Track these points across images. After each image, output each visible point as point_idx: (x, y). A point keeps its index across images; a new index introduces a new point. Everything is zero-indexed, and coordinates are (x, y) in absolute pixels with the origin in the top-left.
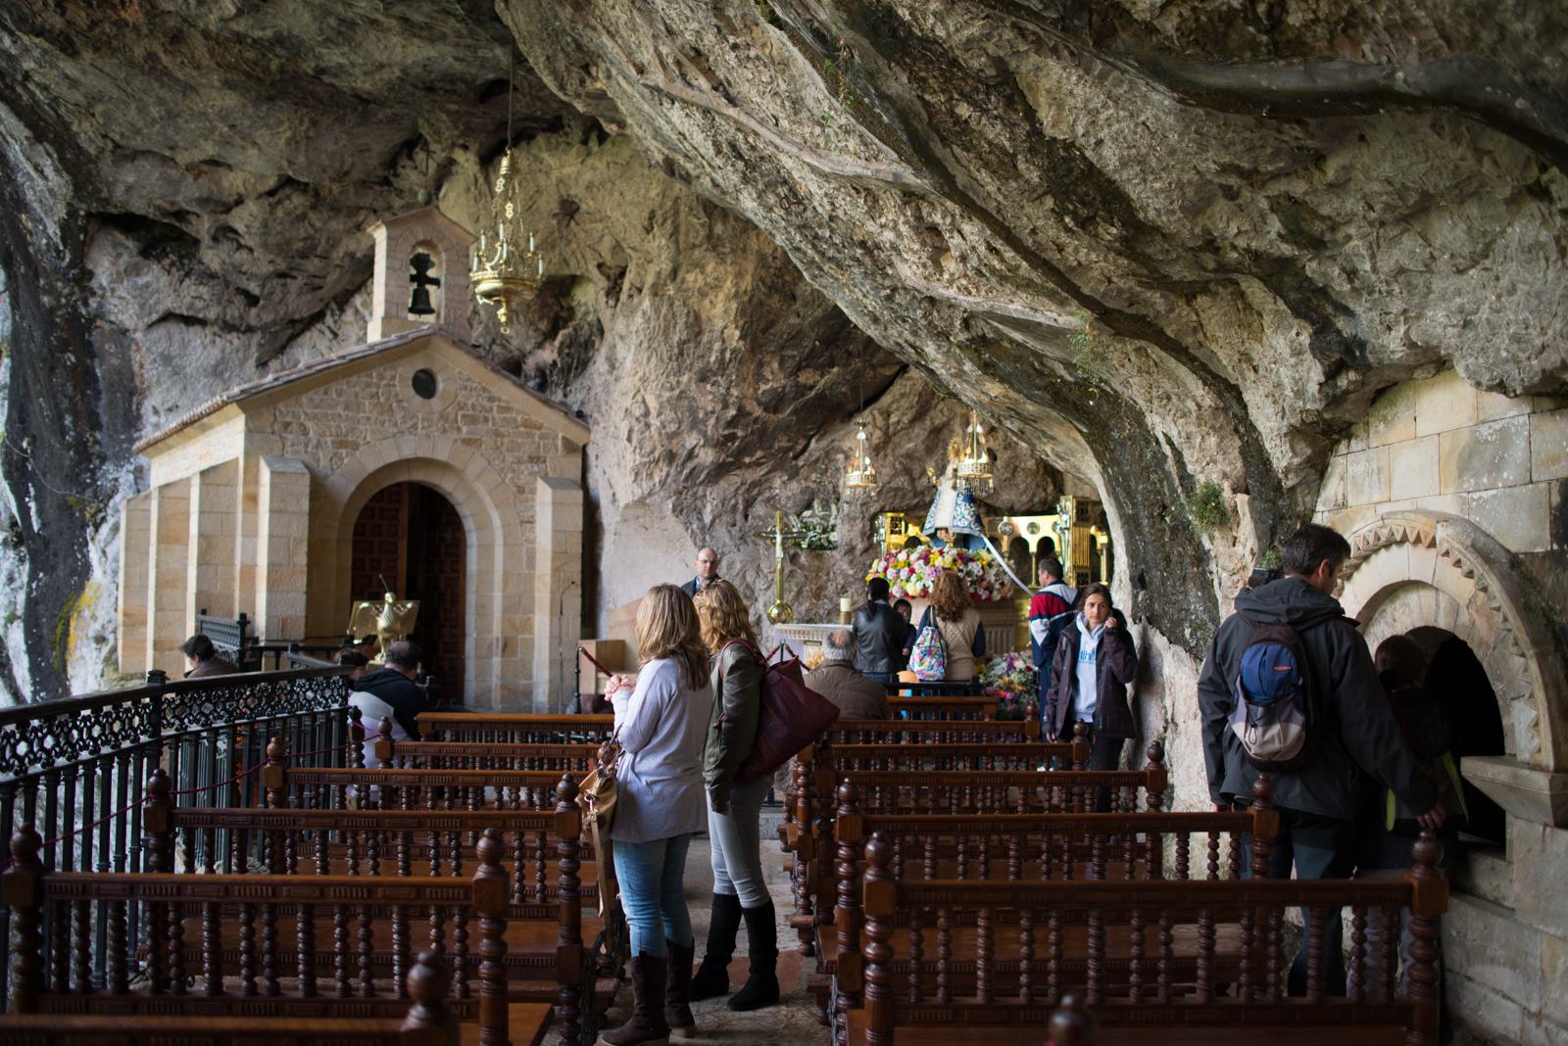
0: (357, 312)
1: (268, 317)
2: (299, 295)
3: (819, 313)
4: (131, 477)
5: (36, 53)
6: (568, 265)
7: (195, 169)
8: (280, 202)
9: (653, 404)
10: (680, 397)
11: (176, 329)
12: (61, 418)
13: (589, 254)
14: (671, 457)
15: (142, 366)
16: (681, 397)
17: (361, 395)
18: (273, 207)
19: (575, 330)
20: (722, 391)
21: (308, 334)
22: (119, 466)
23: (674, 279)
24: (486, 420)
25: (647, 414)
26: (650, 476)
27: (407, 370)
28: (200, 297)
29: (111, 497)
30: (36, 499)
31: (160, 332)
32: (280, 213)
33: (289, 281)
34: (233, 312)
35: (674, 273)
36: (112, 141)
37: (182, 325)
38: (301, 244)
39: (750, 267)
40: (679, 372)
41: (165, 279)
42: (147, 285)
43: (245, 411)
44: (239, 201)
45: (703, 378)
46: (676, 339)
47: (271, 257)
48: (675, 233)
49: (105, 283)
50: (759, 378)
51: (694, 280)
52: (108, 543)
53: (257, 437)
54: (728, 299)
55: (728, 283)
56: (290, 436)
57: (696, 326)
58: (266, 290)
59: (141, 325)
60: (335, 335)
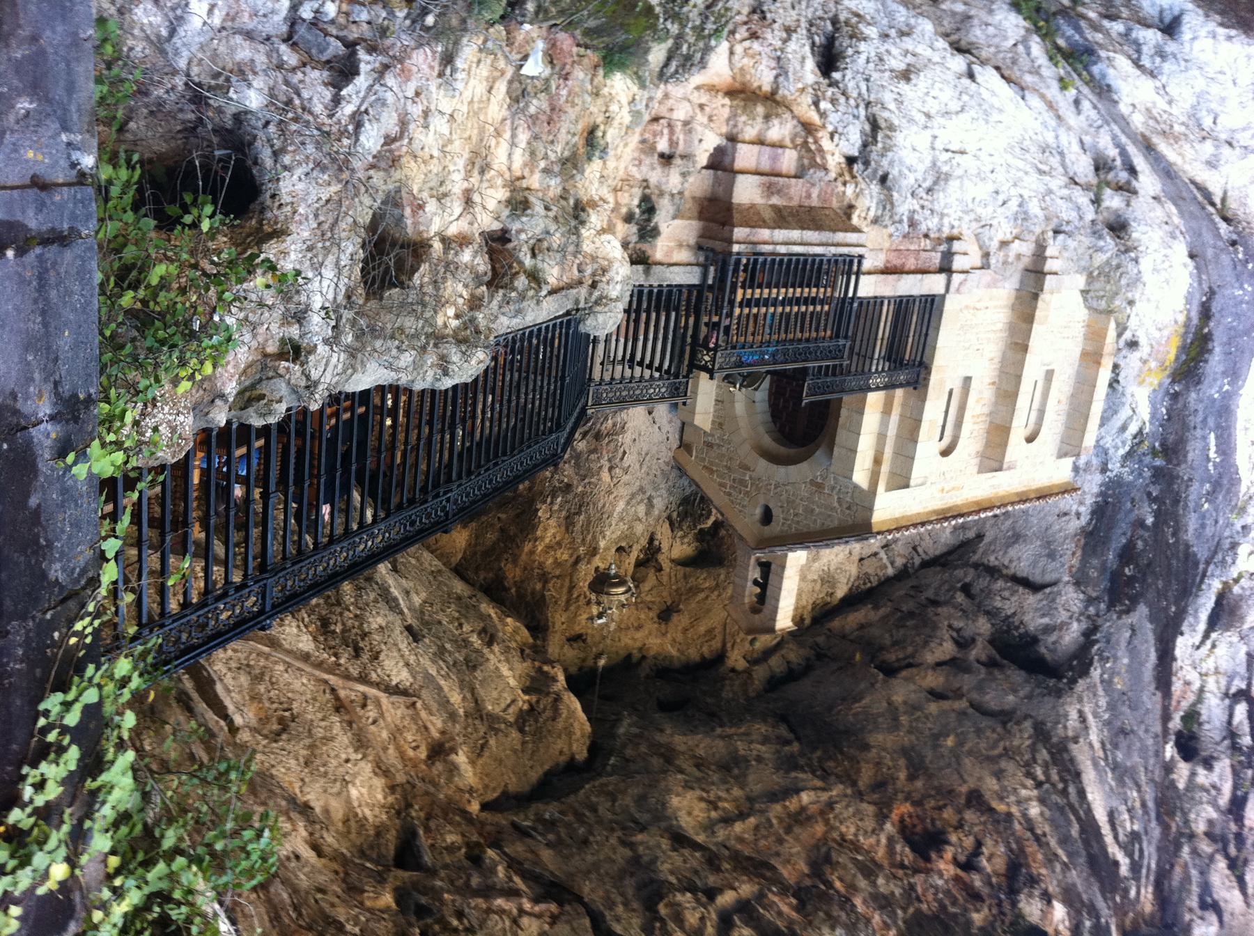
0: (892, 563)
1: (959, 573)
3: (484, 518)
4: (1110, 466)
5: (1012, 799)
7: (958, 694)
8: (905, 659)
9: (605, 476)
11: (1037, 578)
13: (665, 579)
14: (598, 436)
15: (1074, 554)
16: (584, 478)
18: (912, 656)
20: (557, 477)
21: (938, 553)
22: (1119, 476)
24: (734, 480)
25: (611, 469)
26: (614, 425)
28: (1004, 598)
30: (1208, 460)
31: (1048, 578)
32: (910, 649)
33: (932, 597)
34: (983, 582)
37: (1031, 578)
39: (524, 557)
40: (584, 494)
41: (1026, 618)
42: (1043, 616)
44: (939, 664)
45: (568, 487)
46: (582, 517)
47: (935, 618)
48: (572, 588)
49: (1075, 626)
51: (564, 555)
52: (1131, 418)
53: (866, 504)
54: (542, 538)
55: (540, 548)
56: (848, 499)
57: (569, 522)
59: (1061, 586)
60: (915, 548)
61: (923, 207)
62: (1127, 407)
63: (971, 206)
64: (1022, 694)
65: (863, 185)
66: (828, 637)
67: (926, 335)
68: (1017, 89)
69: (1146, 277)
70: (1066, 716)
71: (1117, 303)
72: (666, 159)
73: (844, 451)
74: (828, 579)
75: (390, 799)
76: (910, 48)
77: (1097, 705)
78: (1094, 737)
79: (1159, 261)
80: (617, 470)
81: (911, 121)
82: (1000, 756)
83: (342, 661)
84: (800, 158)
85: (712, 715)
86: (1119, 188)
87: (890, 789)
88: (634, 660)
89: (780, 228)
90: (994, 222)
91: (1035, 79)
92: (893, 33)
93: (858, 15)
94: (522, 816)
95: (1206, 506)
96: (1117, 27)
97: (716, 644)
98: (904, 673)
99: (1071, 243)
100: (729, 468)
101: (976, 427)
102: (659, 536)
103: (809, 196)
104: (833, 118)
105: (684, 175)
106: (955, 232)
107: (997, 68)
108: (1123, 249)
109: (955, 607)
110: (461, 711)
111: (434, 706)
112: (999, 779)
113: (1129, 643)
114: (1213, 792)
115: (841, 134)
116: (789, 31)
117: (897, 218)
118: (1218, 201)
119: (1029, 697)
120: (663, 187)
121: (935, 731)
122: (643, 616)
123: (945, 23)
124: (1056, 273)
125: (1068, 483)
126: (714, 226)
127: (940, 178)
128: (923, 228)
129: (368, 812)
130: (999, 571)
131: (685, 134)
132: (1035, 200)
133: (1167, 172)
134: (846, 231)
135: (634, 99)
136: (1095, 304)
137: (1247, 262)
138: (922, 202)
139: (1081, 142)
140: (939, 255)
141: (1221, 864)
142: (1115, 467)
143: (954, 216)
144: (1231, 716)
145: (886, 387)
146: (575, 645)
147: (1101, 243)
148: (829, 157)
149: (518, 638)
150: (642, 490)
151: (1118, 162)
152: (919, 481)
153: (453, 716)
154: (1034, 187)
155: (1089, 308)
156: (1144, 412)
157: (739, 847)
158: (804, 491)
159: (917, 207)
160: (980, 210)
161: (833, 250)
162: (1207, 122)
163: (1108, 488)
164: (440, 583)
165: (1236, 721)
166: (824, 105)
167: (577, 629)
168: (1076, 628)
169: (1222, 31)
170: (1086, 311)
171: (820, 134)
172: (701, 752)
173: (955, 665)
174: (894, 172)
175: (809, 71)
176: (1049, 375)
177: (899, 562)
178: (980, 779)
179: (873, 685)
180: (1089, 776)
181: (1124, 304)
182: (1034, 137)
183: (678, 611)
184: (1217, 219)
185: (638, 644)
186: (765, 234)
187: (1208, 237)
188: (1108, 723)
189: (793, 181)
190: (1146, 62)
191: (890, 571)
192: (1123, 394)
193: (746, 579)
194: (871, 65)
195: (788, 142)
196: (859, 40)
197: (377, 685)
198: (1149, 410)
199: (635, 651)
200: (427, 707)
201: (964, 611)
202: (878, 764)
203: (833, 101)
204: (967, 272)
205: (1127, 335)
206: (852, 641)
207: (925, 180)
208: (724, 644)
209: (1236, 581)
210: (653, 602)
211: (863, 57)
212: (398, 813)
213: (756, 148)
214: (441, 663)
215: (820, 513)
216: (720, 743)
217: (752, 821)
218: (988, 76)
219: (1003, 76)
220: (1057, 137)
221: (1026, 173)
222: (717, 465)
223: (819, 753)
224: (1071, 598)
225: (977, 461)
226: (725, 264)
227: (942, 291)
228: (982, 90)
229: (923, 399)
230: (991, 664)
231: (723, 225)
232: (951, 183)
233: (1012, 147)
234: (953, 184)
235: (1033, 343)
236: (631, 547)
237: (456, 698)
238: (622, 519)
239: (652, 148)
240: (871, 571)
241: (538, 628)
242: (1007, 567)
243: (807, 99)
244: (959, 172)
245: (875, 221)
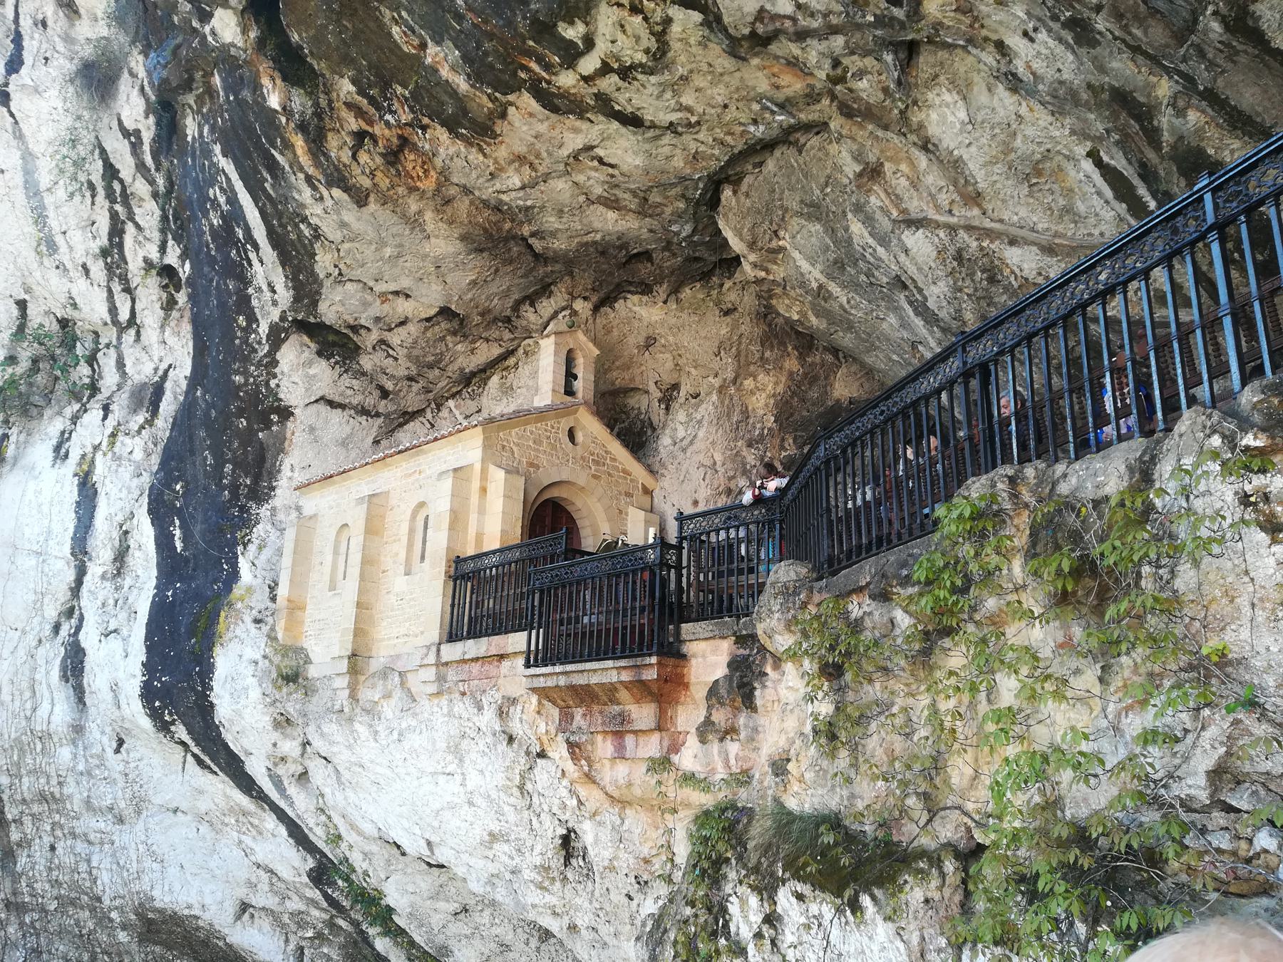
1: (391, 408)
7: (384, 297)
9: (718, 457)
10: (736, 455)
11: (323, 408)
15: (293, 434)
18: (427, 329)
21: (412, 424)
23: (735, 384)
27: (565, 424)
32: (429, 334)
34: (370, 401)
35: (734, 381)
39: (783, 380)
40: (736, 440)
41: (329, 371)
42: (314, 376)
44: (402, 323)
47: (409, 364)
48: (738, 355)
50: (782, 448)
54: (769, 397)
59: (302, 404)
60: (433, 426)
63: (423, 726)
66: (501, 340)
67: (453, 606)
68: (386, 837)
69: (252, 681)
74: (507, 390)
75: (922, 116)
76: (490, 864)
83: (975, 244)
85: (603, 253)
87: (439, 201)
91: (367, 849)
92: (508, 876)
93: (542, 888)
94: (785, 125)
96: (295, 904)
98: (433, 312)
102: (662, 412)
103: (585, 715)
106: (436, 701)
107: (404, 854)
109: (393, 376)
110: (850, 216)
111: (879, 215)
114: (141, 238)
116: (612, 869)
122: (671, 338)
123: (453, 890)
129: (947, 97)
130: (357, 413)
134: (544, 688)
138: (471, 724)
145: (486, 554)
146: (730, 306)
149: (787, 301)
150: (684, 450)
151: (286, 783)
152: (444, 476)
153: (859, 208)
154: (365, 750)
156: (243, 564)
157: (578, 123)
160: (414, 723)
162: (204, 829)
164: (867, 341)
165: (129, 304)
167: (728, 319)
169: (196, 912)
171: (576, 775)
172: (612, 215)
175: (588, 834)
176: (332, 587)
177: (444, 413)
182: (367, 796)
190: (265, 876)
191: (451, 403)
194: (529, 844)
196: (542, 866)
197: (938, 225)
200: (886, 213)
203: (564, 806)
205: (265, 629)
211: (538, 849)
212: (915, 103)
214: (872, 260)
216: (597, 225)
217: (565, 152)
218: (414, 846)
219: (398, 847)
222: (620, 477)
226: (661, 645)
228: (418, 832)
230: (355, 328)
235: (351, 611)
237: (857, 227)
238: (699, 422)
241: (766, 314)
243: (590, 806)
245: (514, 701)
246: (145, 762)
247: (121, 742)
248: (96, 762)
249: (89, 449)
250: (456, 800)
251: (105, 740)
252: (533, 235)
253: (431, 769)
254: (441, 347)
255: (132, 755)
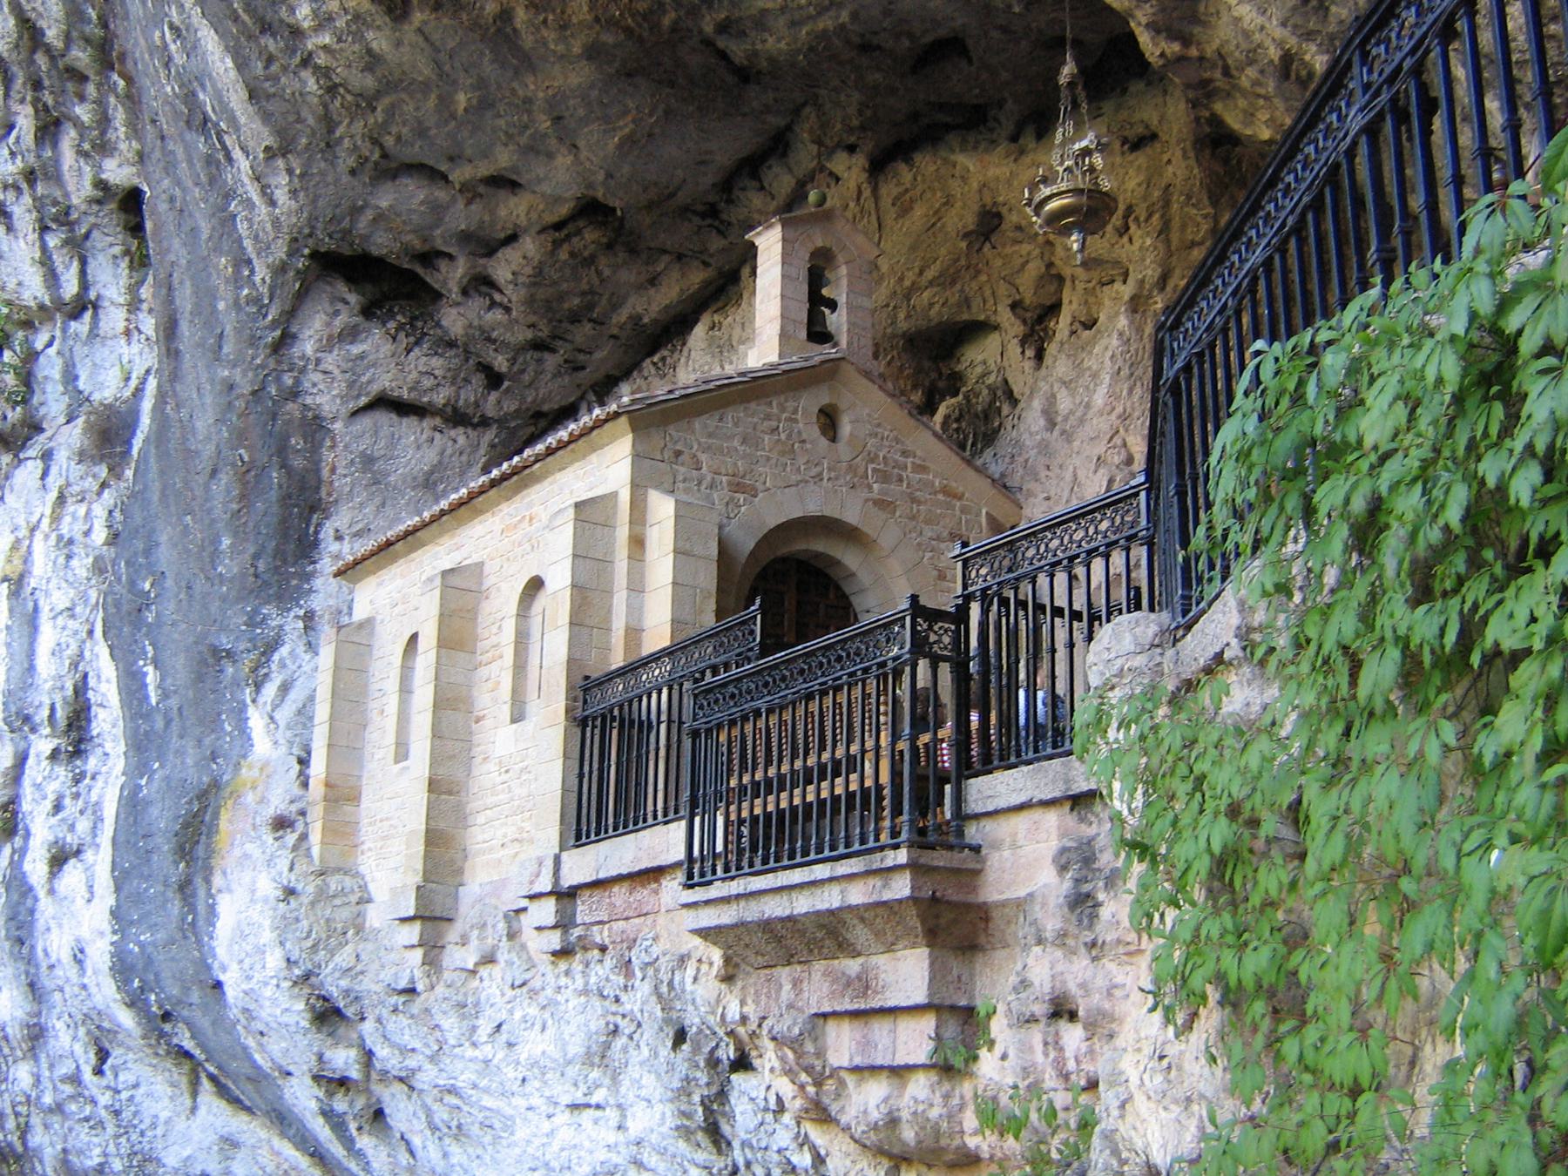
1: (510, 406)
2: (554, 376)
4: (301, 624)
5: (340, 23)
6: (969, 307)
7: (470, 191)
8: (568, 237)
11: (384, 418)
12: (216, 541)
13: (1003, 289)
15: (333, 470)
17: (760, 428)
18: (557, 244)
19: (967, 397)
23: (1162, 289)
24: (900, 480)
29: (274, 650)
30: (156, 663)
31: (366, 421)
32: (563, 255)
33: (546, 355)
34: (468, 395)
36: (382, 147)
37: (394, 416)
38: (576, 301)
41: (387, 348)
42: (362, 356)
43: (634, 429)
44: (512, 239)
47: (532, 319)
48: (1165, 230)
52: (275, 707)
56: (682, 469)
58: (515, 369)
59: (344, 412)
61: (617, 1000)
62: (282, 724)
63: (547, 1015)
64: (369, 215)
65: (711, 1020)
67: (581, 776)
69: (268, 936)
70: (293, 193)
71: (311, 889)
72: (1062, 1010)
73: (698, 550)
77: (249, 220)
78: (244, 164)
79: (257, 967)
80: (1117, 460)
81: (662, 1152)
82: (378, 94)
84: (820, 1054)
85: (866, 48)
86: (343, 1082)
88: (1029, 133)
89: (831, 912)
90: (510, 993)
95: (147, 586)
97: (888, 190)
98: (564, 210)
99: (387, 975)
100: (914, 500)
101: (494, 640)
102: (1028, 365)
103: (796, 983)
104: (783, 1138)
105: (1024, 984)
106: (563, 965)
108: (313, 979)
112: (369, 51)
113: (221, 335)
114: (87, 146)
115: (766, 1109)
117: (650, 971)
118: (206, 1084)
119: (356, 211)
120: (1059, 953)
121: (489, 114)
124: (404, 920)
125: (355, 581)
126: (953, 895)
127: (600, 1055)
128: (609, 962)
130: (447, 420)
131: (1034, 1065)
132: (452, 1042)
133: (282, 1119)
134: (719, 929)
135: (1122, 1106)
136: (348, 882)
137: (142, 989)
139: (412, 1153)
140: (579, 921)
141: (52, 35)
142: (293, 626)
143: (568, 993)
144: (83, 273)
146: (1140, 130)
147: (344, 983)
148: (777, 1064)
149: (1242, 103)
150: (1068, 436)
151: (353, 1126)
154: (460, 1065)
155: (357, 875)
156: (256, 721)
158: (766, 474)
159: (624, 998)
160: (533, 1011)
161: (735, 887)
163: (299, 587)
166: (803, 1160)
167: (1141, 158)
168: (307, 346)
170: (362, 869)
171: (798, 1103)
173: (488, 245)
174: (665, 1051)
176: (402, 752)
178: (398, 44)
179: (609, 176)
180: (237, 99)
181: (299, 887)
182: (480, 1151)
183: (966, 235)
184: (197, 1052)
185: (1027, 159)
186: (858, 895)
187: (204, 1023)
188: (228, 196)
189: (827, 1008)
192: (291, 743)
193: (851, 308)
195: (850, 1080)
198: (251, 723)
199: (1032, 145)
201: (489, 340)
202: (564, 27)
204: (532, 897)
205: (291, 838)
206: (665, 252)
207: (625, 1050)
208: (875, 190)
209: (104, 485)
210: (1016, 242)
213: (900, 1060)
215: (731, 438)
220: (445, 1155)
221: (475, 1086)
223: (667, 21)
224: (326, 396)
225: (487, 583)
227: (565, 856)
229: (572, 662)
230: (429, 257)
231: (934, 899)
232: (582, 1050)
233: (505, 1128)
234: (576, 1048)
235: (418, 798)
236: (1073, 333)
238: (1095, 376)
239: (1091, 1028)
240: (656, 382)
242: (435, 429)
244: (572, 1071)
245: (683, 960)
246: (142, 1090)
247: (103, 1055)
248: (68, 1089)
249: (23, 533)
250: (616, 1159)
251: (78, 1048)
252: (723, 28)
253: (566, 1100)
254: (588, 278)
255: (121, 1078)
